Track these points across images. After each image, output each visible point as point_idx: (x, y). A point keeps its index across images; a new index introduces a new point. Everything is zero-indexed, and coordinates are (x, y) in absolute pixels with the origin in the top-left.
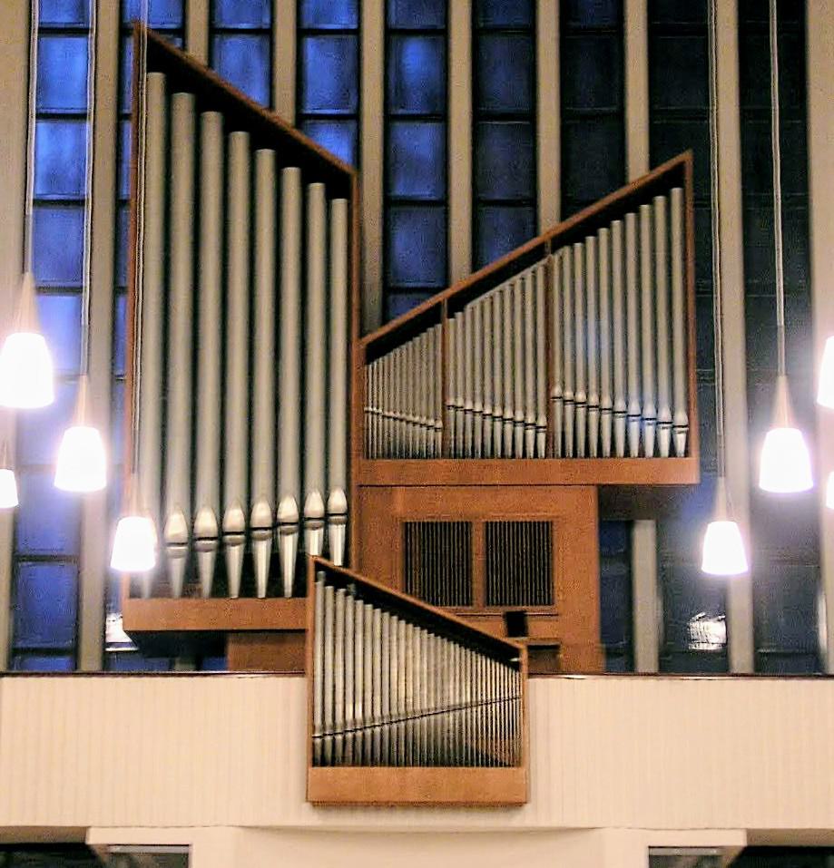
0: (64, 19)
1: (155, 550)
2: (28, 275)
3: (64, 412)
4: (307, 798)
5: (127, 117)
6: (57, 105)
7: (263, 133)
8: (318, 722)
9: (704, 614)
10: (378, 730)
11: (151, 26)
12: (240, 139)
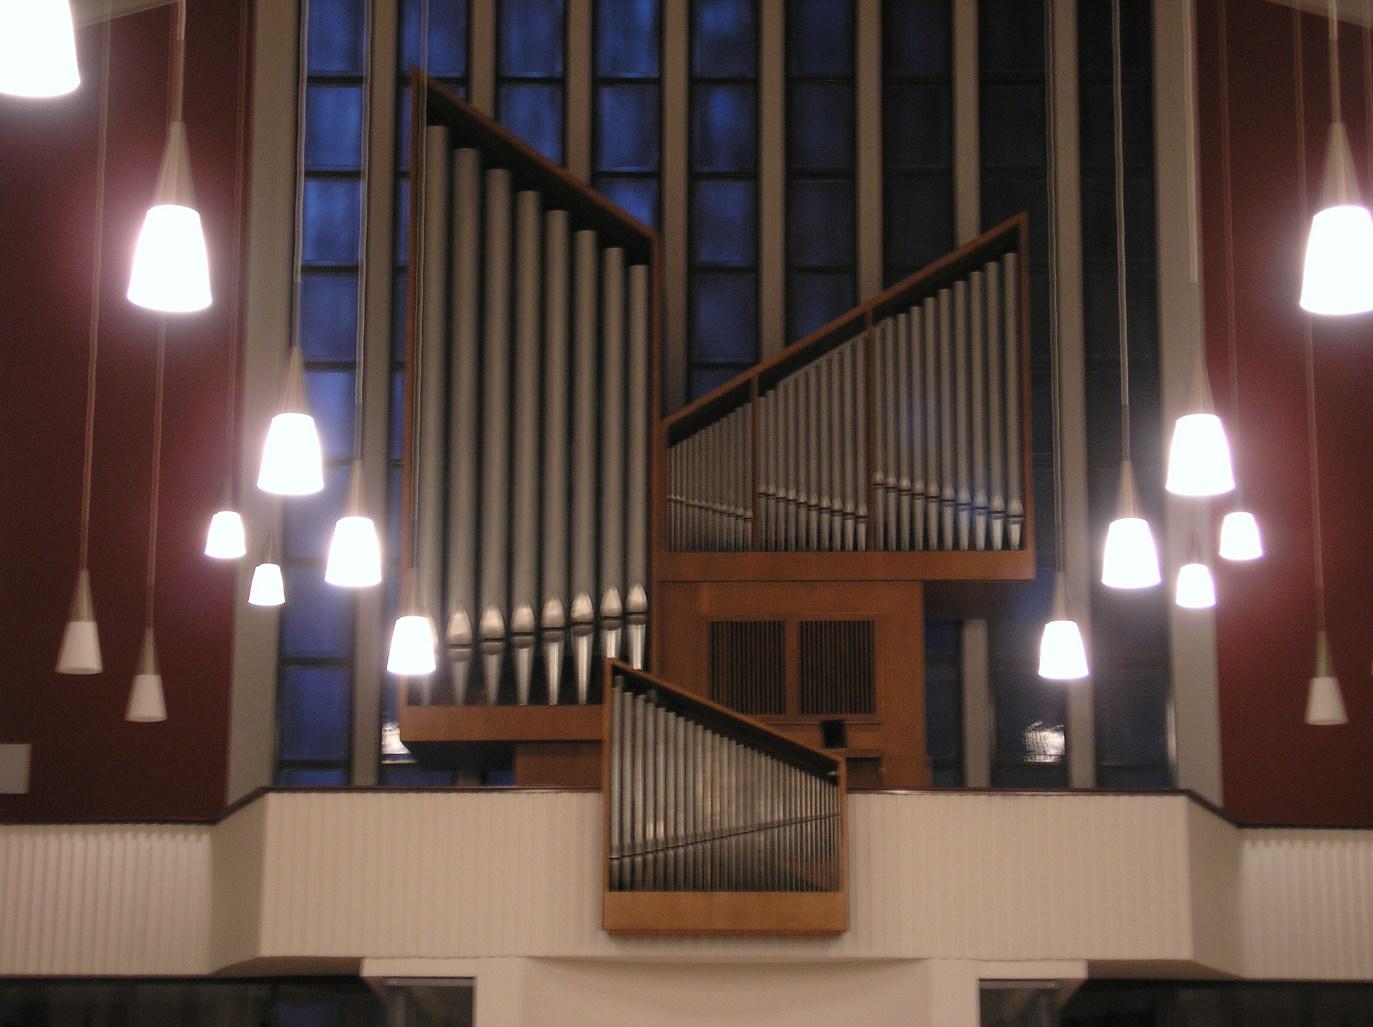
0: (336, 66)
1: (436, 652)
2: (296, 351)
3: (331, 504)
4: (603, 926)
5: (405, 174)
6: (328, 162)
7: (555, 193)
8: (616, 841)
9: (1041, 723)
10: (681, 851)
11: (431, 74)
12: (530, 200)
